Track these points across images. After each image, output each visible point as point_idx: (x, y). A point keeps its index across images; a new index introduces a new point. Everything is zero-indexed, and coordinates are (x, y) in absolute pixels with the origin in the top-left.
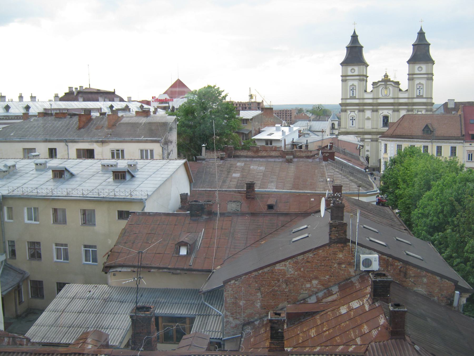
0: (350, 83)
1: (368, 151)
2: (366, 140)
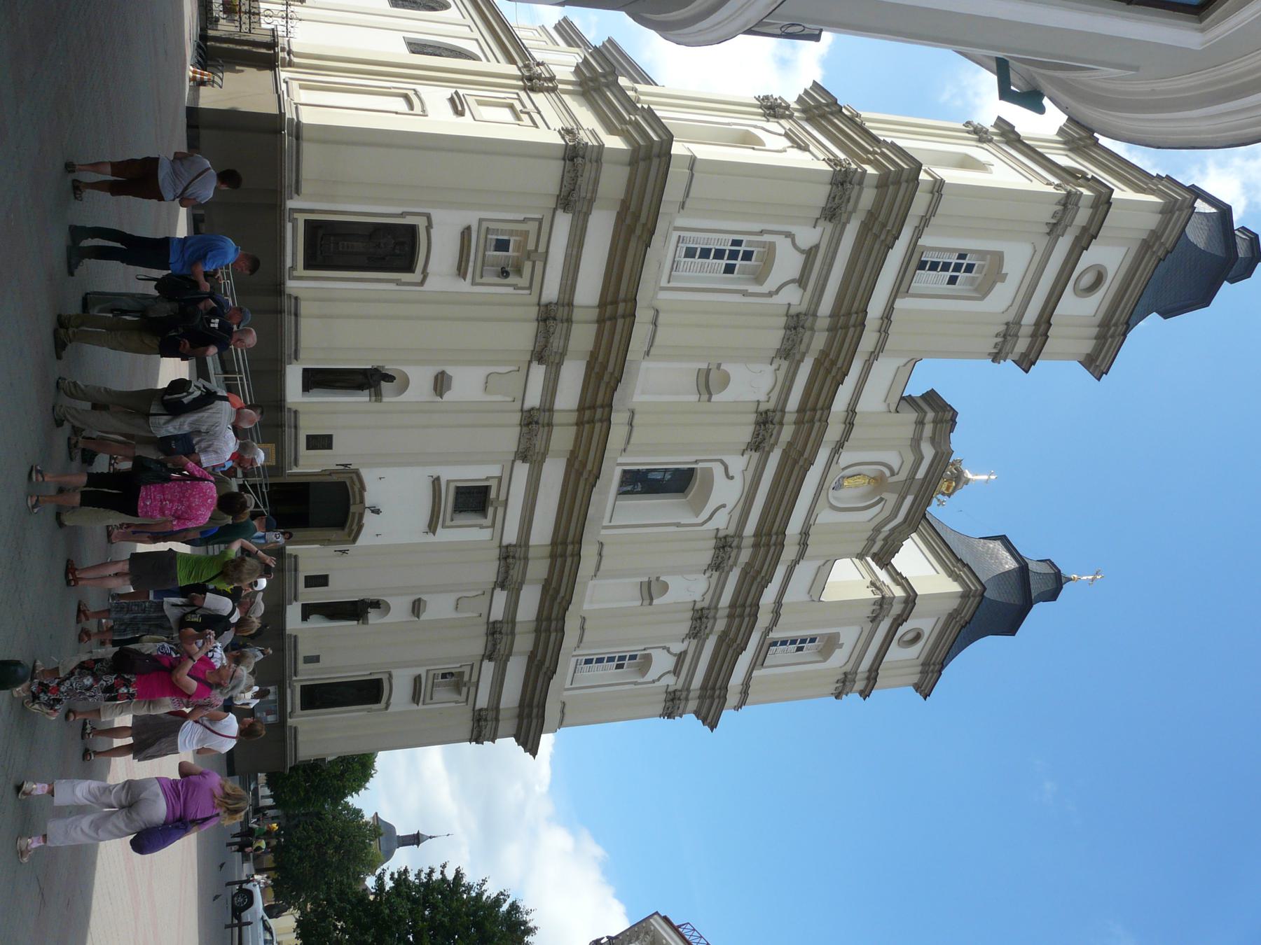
1: (441, 383)
2: (538, 373)
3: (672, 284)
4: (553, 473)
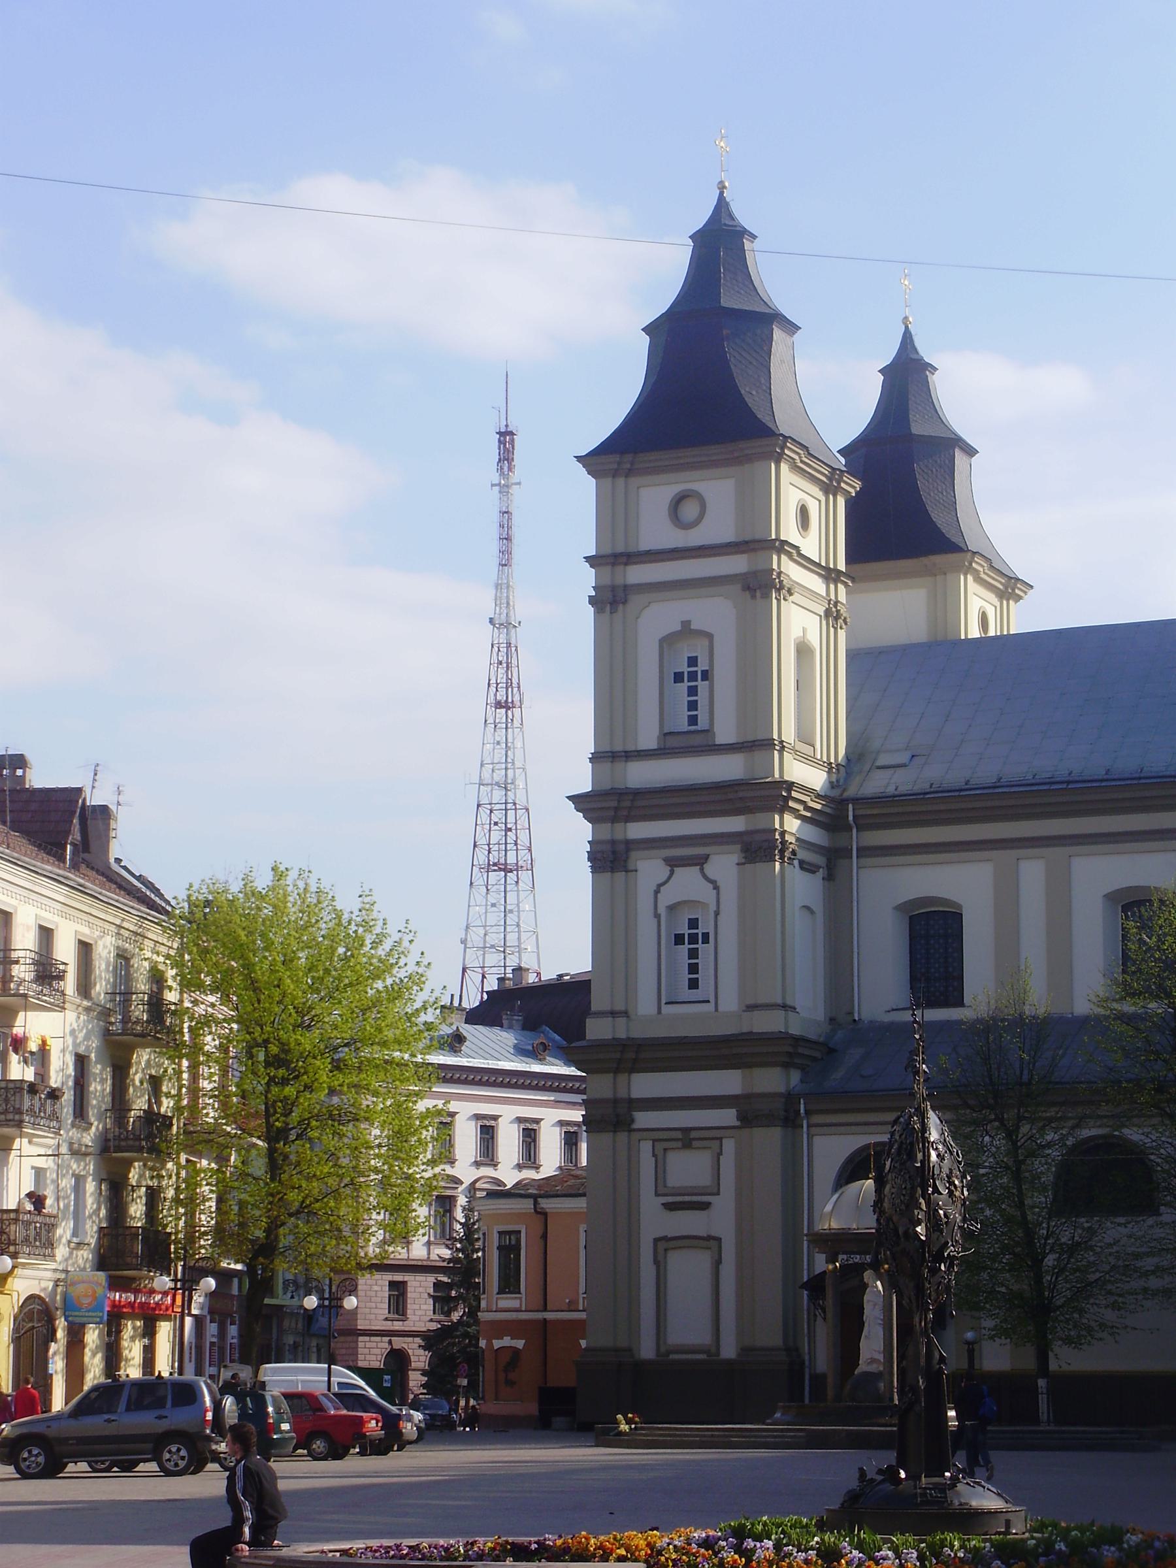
0: (656, 619)
3: (712, 999)
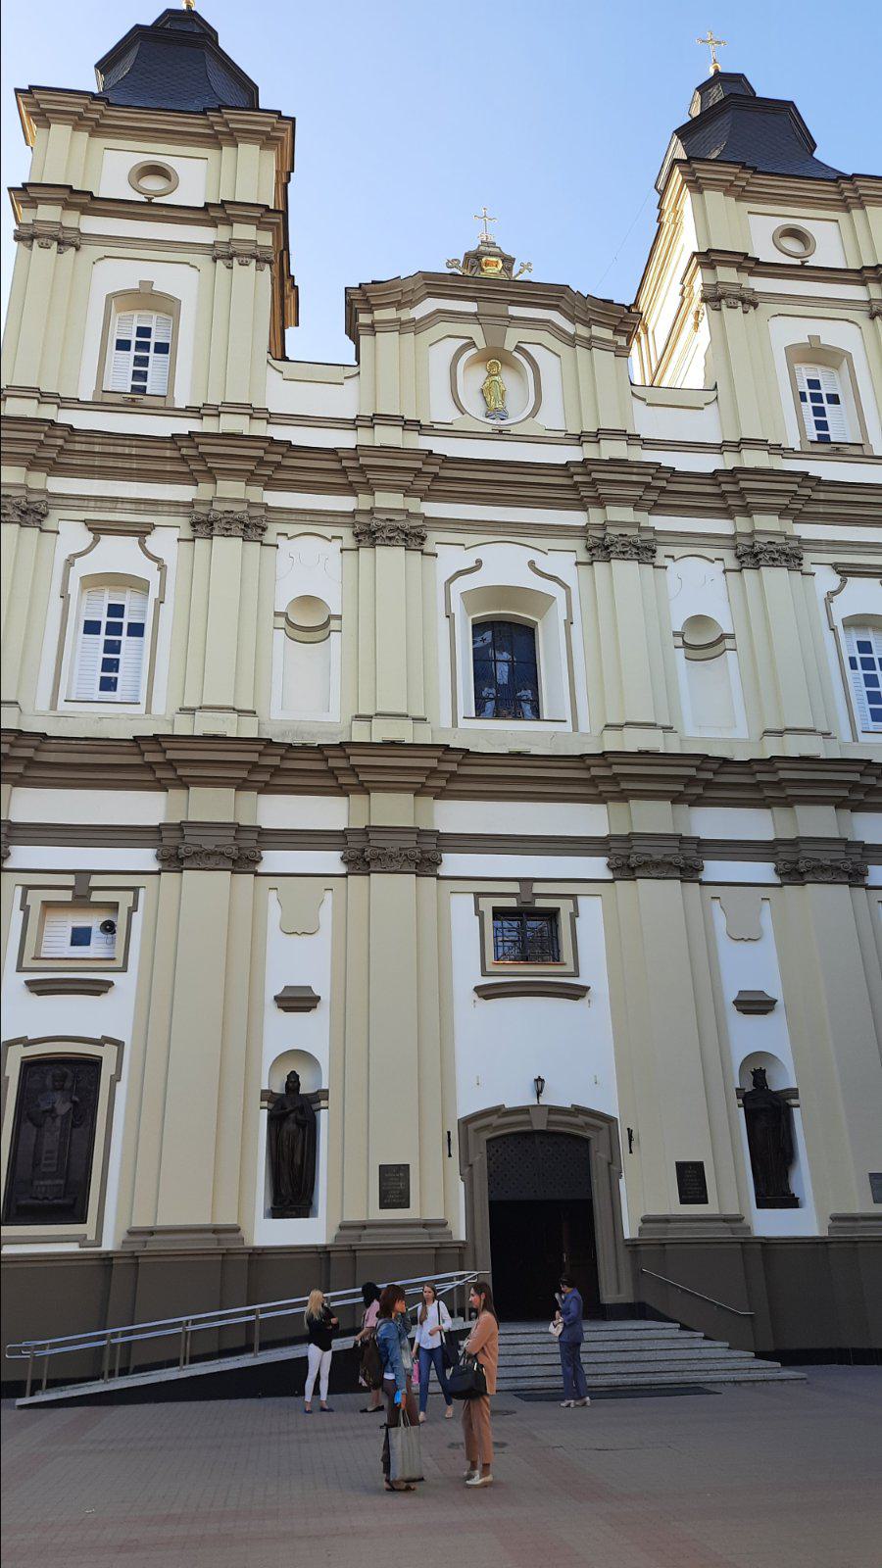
1: (297, 1001)
2: (274, 860)
3: (143, 700)
4: (454, 816)
